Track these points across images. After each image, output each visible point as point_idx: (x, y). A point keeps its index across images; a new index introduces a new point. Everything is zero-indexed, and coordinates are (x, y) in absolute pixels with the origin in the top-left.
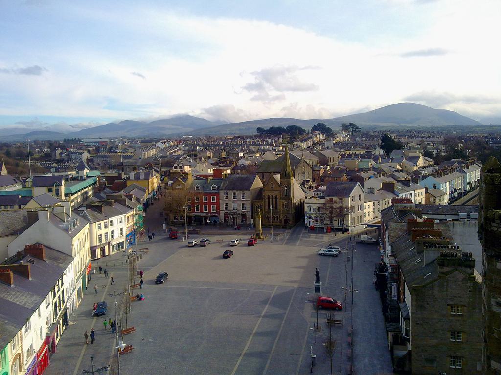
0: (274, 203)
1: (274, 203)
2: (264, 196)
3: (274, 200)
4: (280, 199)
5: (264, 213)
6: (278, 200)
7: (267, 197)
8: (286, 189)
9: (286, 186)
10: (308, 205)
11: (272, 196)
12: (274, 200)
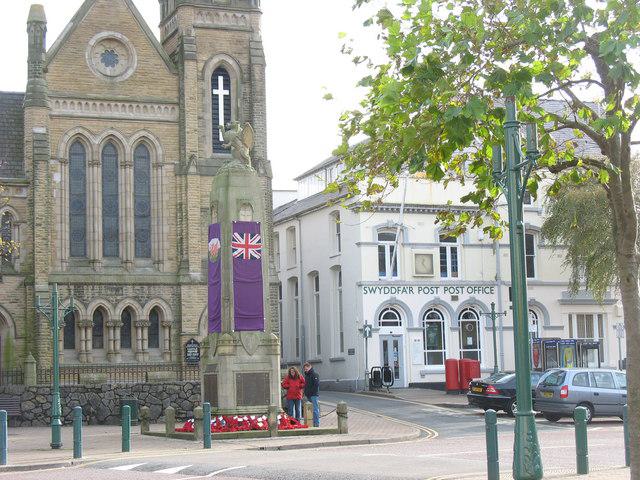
0: (127, 203)
1: (127, 203)
2: (41, 141)
3: (127, 176)
4: (181, 171)
5: (41, 284)
6: (163, 179)
7: (63, 151)
8: (221, 92)
9: (221, 70)
10: (381, 219)
11: (111, 144)
12: (127, 176)
